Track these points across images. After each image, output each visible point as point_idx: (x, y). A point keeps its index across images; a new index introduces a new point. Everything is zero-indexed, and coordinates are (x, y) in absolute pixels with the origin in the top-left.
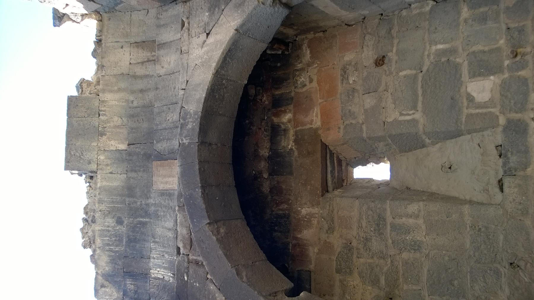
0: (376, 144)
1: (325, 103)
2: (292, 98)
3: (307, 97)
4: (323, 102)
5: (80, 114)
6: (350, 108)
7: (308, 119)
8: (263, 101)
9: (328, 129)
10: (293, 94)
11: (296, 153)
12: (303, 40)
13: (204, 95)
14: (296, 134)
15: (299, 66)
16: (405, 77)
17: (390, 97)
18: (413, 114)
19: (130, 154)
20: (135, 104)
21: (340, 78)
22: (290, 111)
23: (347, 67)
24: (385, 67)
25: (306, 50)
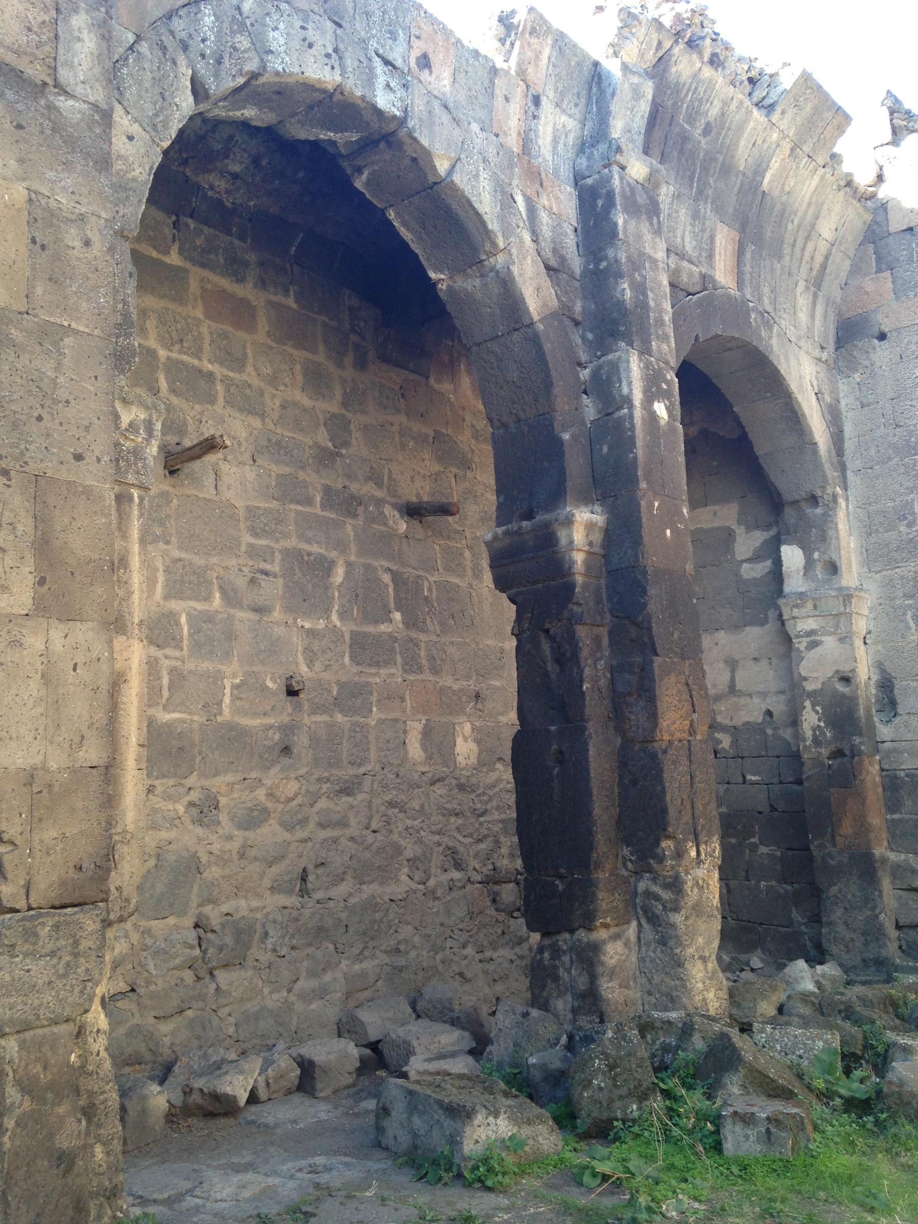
5: (829, 127)
13: (782, 371)
19: (756, 189)
20: (790, 226)
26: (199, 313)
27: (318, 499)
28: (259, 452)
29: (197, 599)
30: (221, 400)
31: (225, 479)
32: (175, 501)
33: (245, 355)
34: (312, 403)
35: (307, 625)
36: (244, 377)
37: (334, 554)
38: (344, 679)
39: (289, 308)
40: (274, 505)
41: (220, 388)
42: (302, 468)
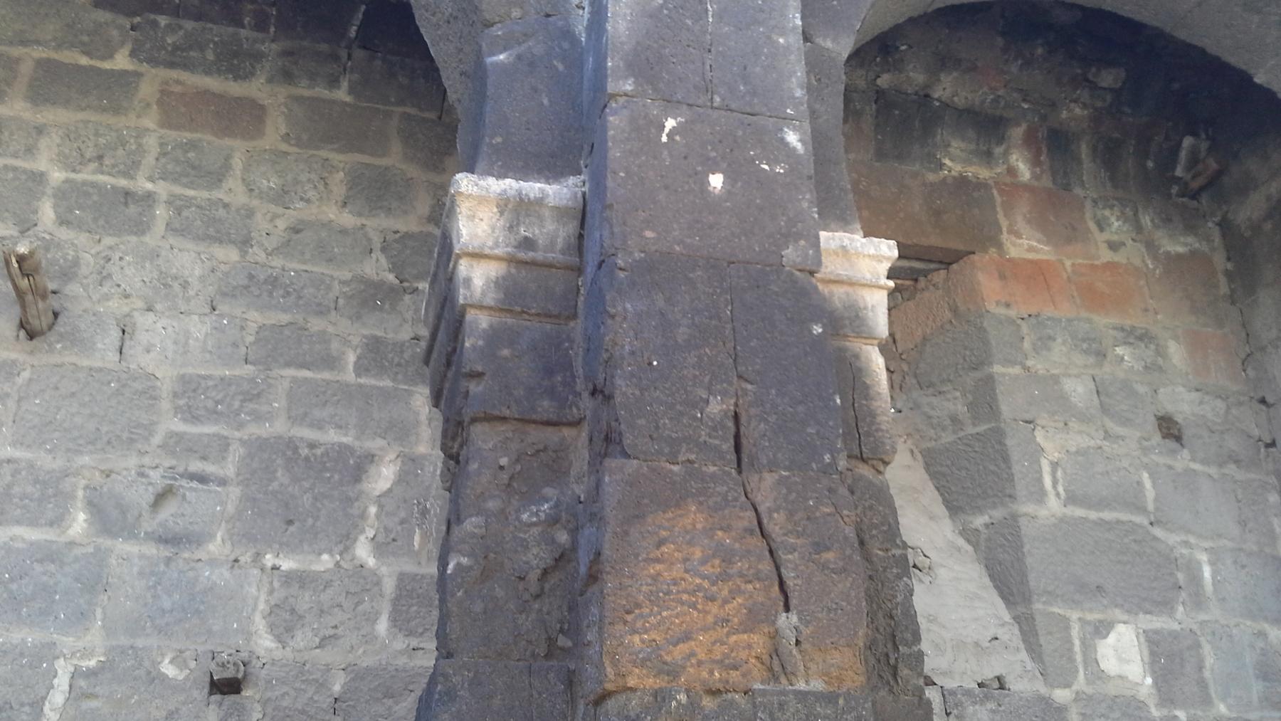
0: (958, 394)
1: (1065, 276)
2: (1067, 188)
3: (1074, 229)
4: (1065, 269)
6: (1059, 340)
7: (1021, 224)
8: (1072, 105)
9: (1002, 277)
10: (1078, 191)
11: (931, 177)
12: (1209, 240)
14: (981, 185)
15: (1146, 220)
16: (1138, 483)
17: (1092, 443)
18: (1058, 495)
21: (1128, 323)
22: (1035, 177)
23: (1152, 347)
24: (1157, 438)
25: (1186, 245)
26: (149, 122)
27: (351, 358)
28: (224, 294)
29: (33, 523)
30: (160, 227)
31: (143, 337)
32: (26, 375)
33: (227, 167)
34: (359, 221)
35: (287, 564)
36: (218, 194)
37: (375, 444)
38: (367, 662)
39: (334, 102)
40: (249, 369)
41: (161, 212)
42: (320, 313)
